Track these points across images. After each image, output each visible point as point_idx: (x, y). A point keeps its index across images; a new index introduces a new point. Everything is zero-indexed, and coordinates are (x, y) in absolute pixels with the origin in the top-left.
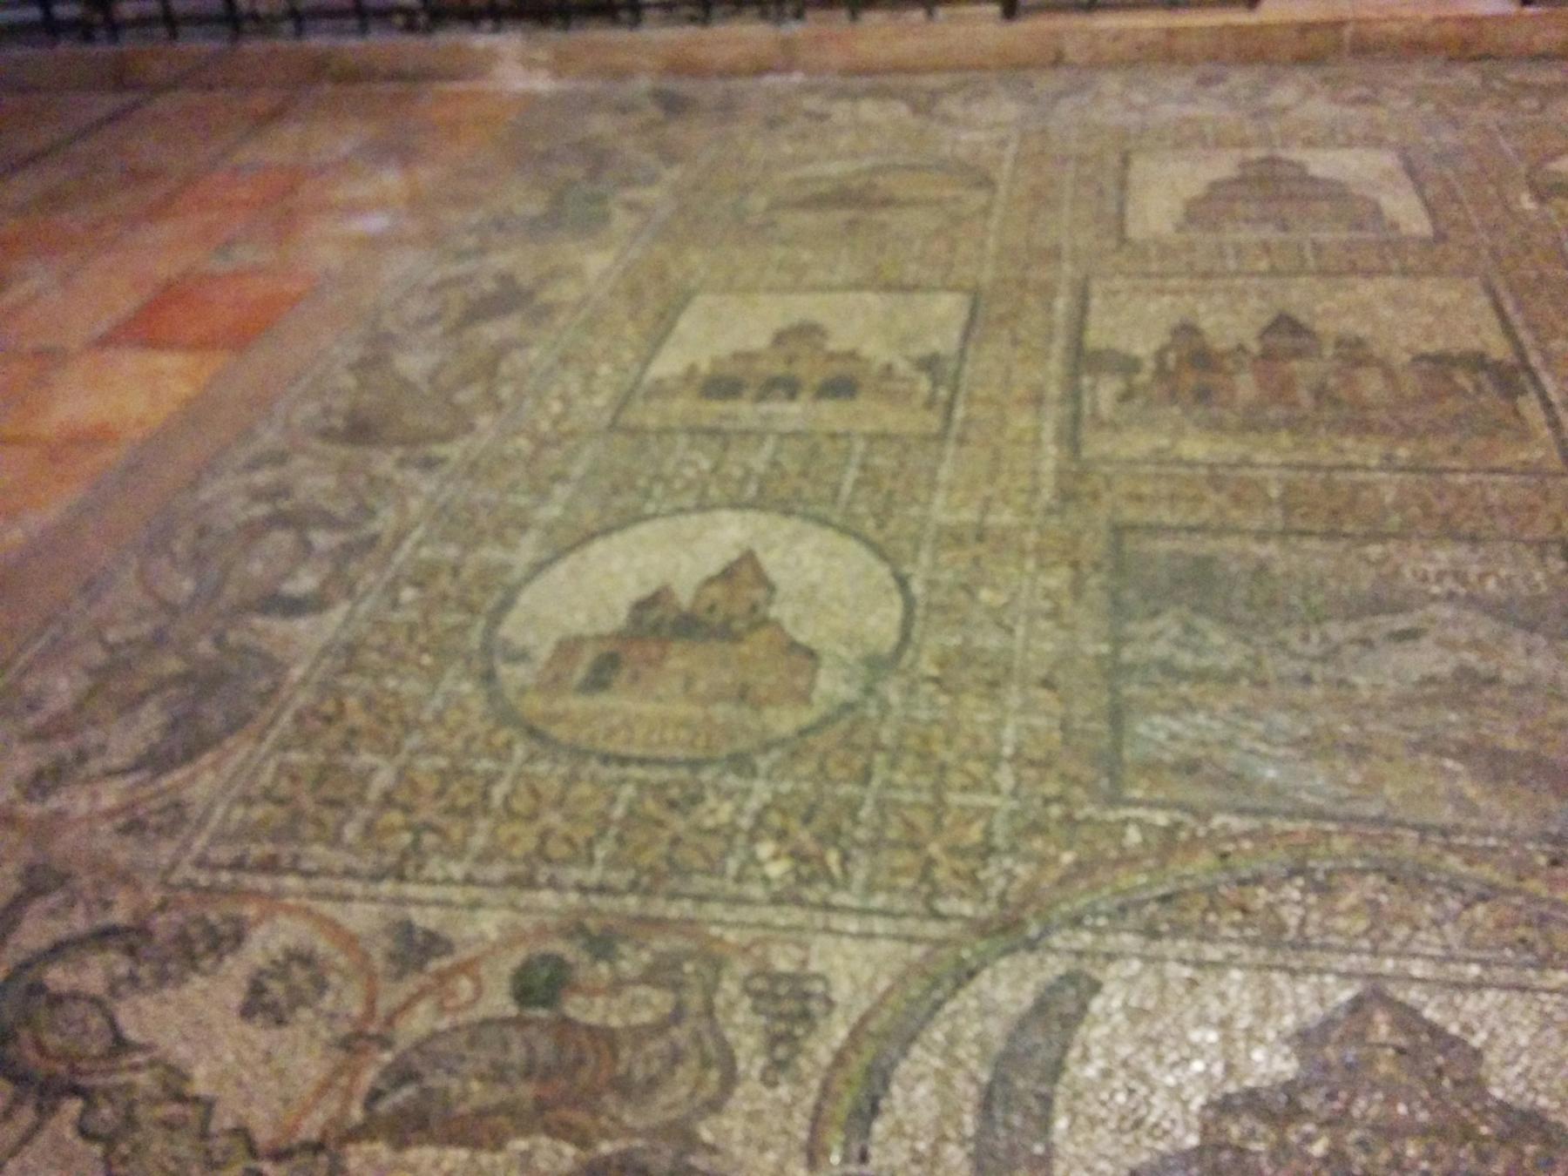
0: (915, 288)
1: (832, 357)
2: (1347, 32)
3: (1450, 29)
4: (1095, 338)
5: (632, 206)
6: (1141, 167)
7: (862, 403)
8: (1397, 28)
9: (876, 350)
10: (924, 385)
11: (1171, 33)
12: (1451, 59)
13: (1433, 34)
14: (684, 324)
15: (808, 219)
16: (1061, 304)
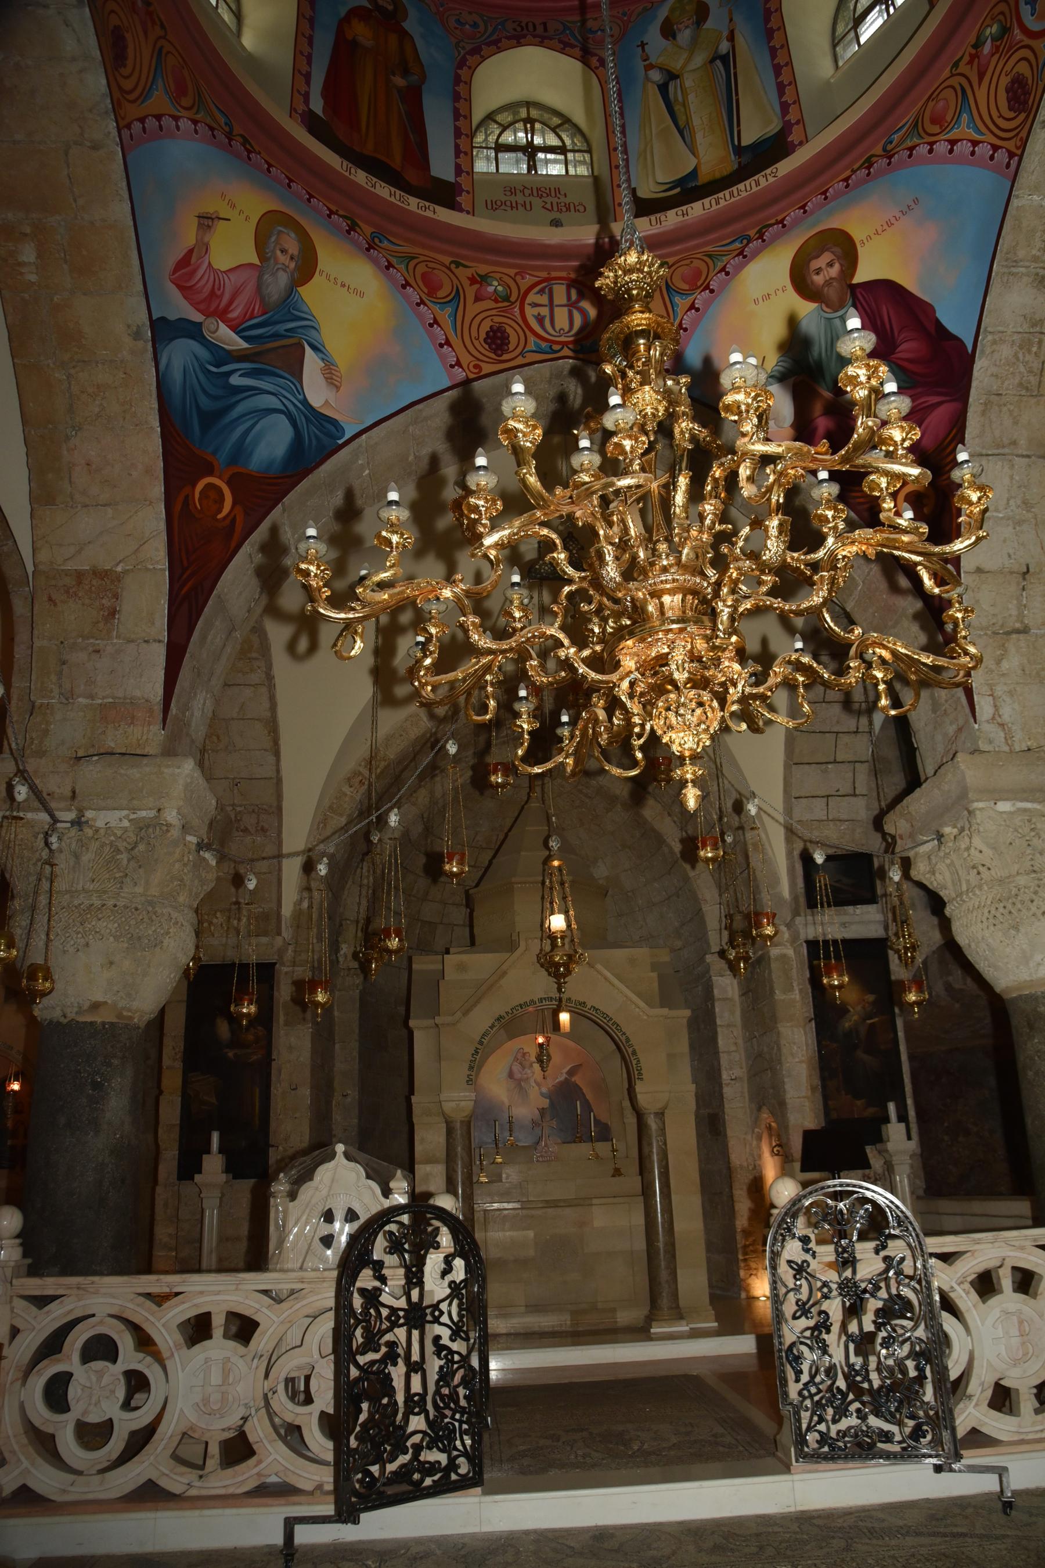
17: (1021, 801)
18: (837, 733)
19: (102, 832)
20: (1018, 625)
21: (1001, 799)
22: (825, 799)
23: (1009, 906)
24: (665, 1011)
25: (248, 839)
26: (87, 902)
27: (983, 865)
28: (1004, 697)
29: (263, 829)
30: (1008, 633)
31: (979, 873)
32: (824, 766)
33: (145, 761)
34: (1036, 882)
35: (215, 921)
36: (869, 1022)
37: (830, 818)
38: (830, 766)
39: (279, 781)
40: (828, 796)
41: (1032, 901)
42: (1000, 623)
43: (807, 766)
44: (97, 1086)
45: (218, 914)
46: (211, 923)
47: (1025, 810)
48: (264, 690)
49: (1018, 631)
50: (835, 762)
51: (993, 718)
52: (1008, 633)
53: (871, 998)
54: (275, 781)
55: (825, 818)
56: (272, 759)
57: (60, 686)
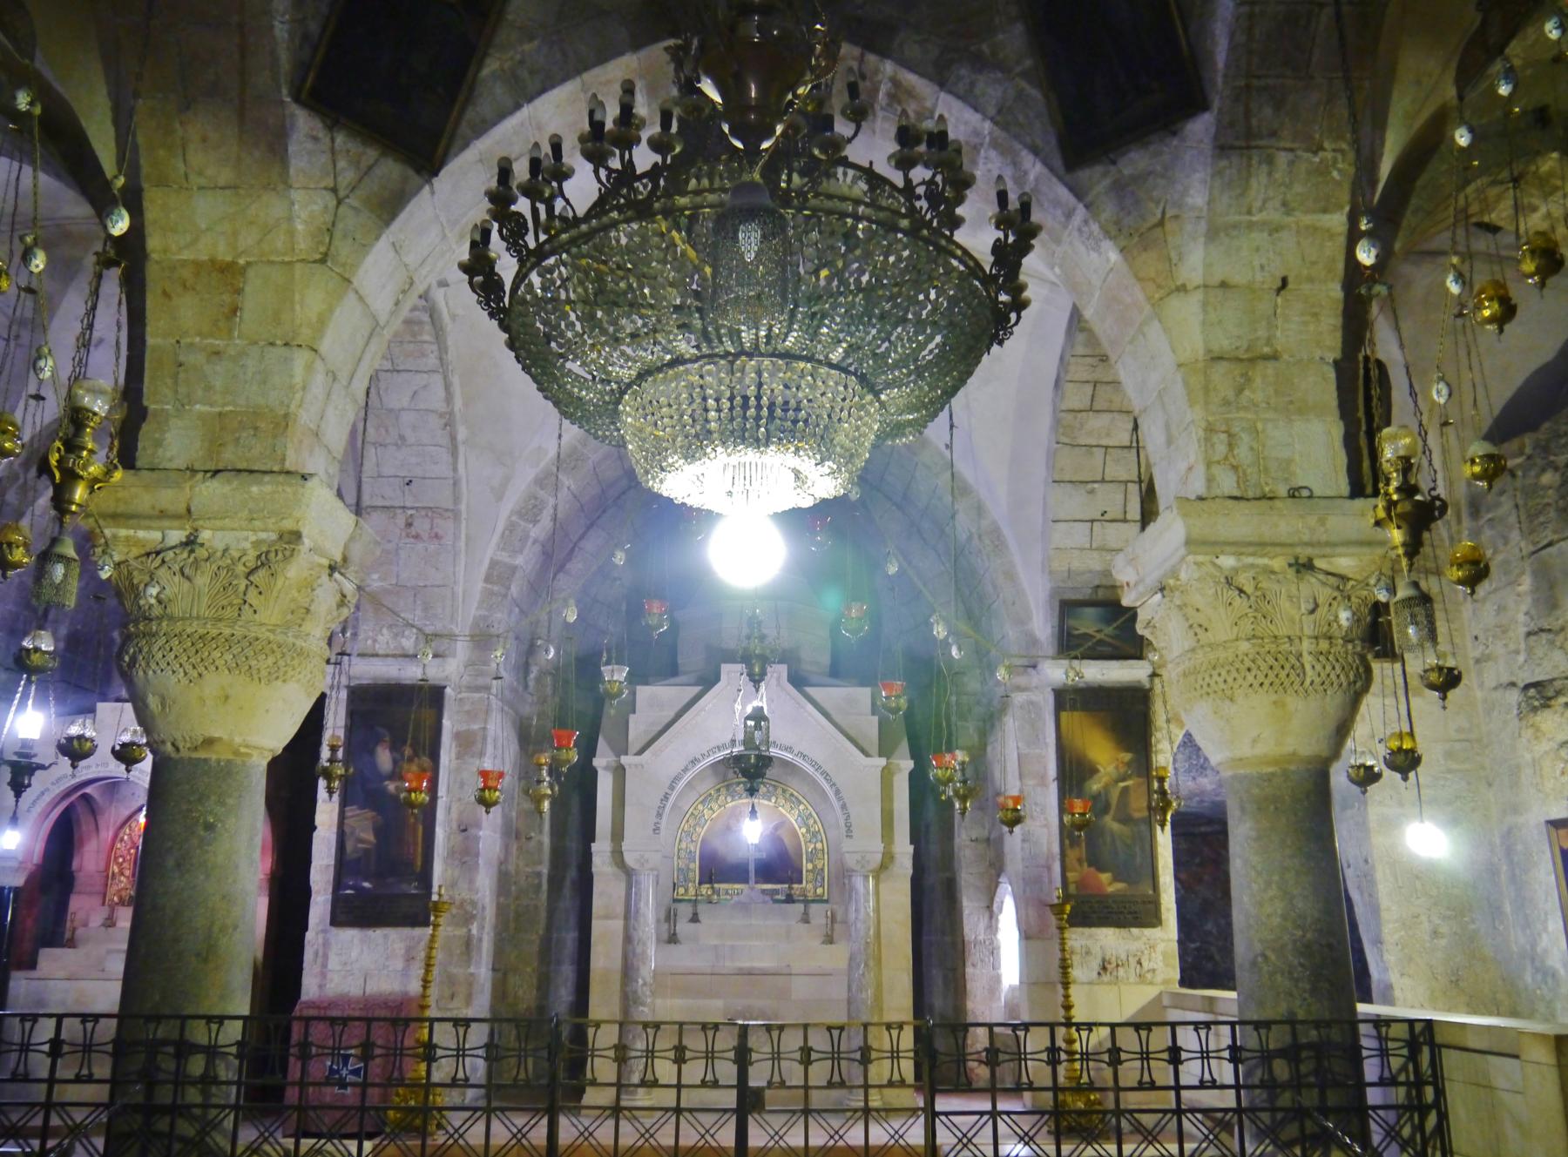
17: (1253, 554)
18: (1107, 447)
19: (219, 554)
20: (1266, 350)
21: (1222, 552)
22: (1089, 524)
23: (1224, 673)
24: (883, 761)
25: (420, 546)
26: (202, 631)
27: (1200, 626)
28: (1243, 435)
29: (437, 536)
30: (1252, 360)
31: (1196, 634)
32: (1090, 486)
33: (267, 478)
34: (1257, 649)
35: (380, 638)
36: (1122, 784)
37: (1094, 546)
38: (1096, 485)
39: (456, 483)
40: (1092, 521)
41: (1249, 670)
42: (1245, 346)
43: (1069, 485)
44: (210, 827)
45: (385, 631)
46: (375, 641)
47: (1252, 566)
48: (437, 379)
49: (1266, 358)
50: (1103, 481)
51: (1226, 458)
52: (1252, 360)
53: (1127, 756)
54: (451, 482)
55: (1088, 546)
56: (445, 457)
57: (176, 392)
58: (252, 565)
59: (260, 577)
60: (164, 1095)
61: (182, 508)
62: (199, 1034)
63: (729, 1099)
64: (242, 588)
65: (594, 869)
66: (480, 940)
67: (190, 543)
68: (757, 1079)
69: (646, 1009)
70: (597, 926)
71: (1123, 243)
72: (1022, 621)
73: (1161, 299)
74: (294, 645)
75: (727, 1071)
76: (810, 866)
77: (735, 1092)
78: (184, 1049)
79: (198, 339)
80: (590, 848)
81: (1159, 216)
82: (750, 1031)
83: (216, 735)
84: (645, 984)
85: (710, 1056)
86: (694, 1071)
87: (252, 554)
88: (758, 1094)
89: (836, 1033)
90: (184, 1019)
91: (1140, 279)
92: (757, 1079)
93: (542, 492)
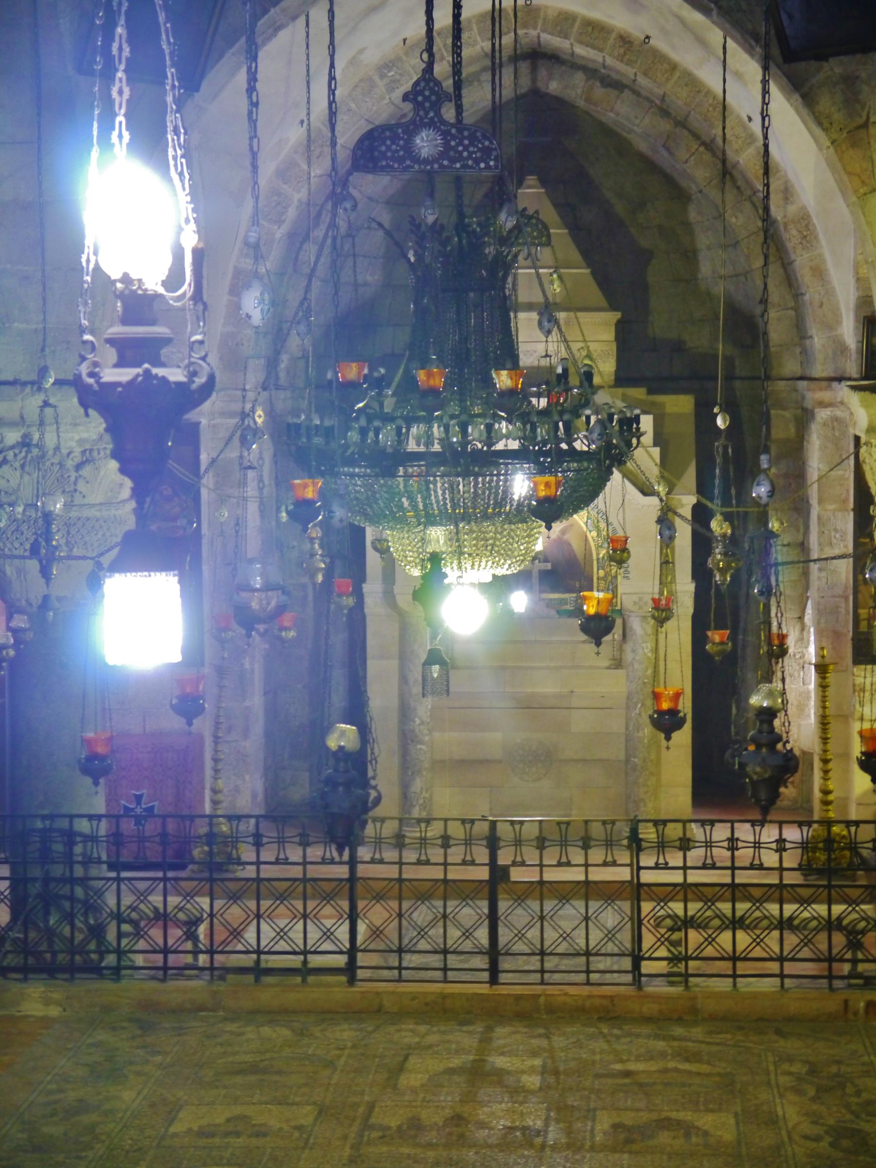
0: (293, 1104)
1: (254, 1125)
2: (542, 1000)
3: (597, 1002)
4: (373, 1121)
5: (138, 1074)
6: (413, 1061)
7: (269, 1139)
8: (569, 1000)
9: (274, 1123)
10: (296, 1134)
11: (444, 997)
12: (600, 1019)
13: (588, 1004)
14: (181, 1115)
15: (239, 1079)
16: (361, 1109)
19: (51, 452)
58: (78, 460)
59: (86, 471)
60: (57, 871)
61: (16, 416)
62: (83, 826)
63: (483, 874)
64: (73, 479)
65: (366, 610)
66: (252, 671)
67: (25, 443)
68: (504, 858)
69: (424, 747)
70: (373, 666)
71: (835, 136)
72: (832, 324)
73: (865, 194)
74: (115, 516)
75: (482, 854)
76: (602, 573)
77: (487, 868)
78: (70, 837)
79: (9, 266)
80: (361, 589)
81: (864, 118)
82: (499, 825)
83: (62, 595)
84: (422, 723)
85: (468, 842)
86: (456, 854)
87: (78, 451)
88: (505, 870)
89: (563, 827)
90: (72, 817)
91: (849, 174)
92: (504, 858)
93: (285, 187)
